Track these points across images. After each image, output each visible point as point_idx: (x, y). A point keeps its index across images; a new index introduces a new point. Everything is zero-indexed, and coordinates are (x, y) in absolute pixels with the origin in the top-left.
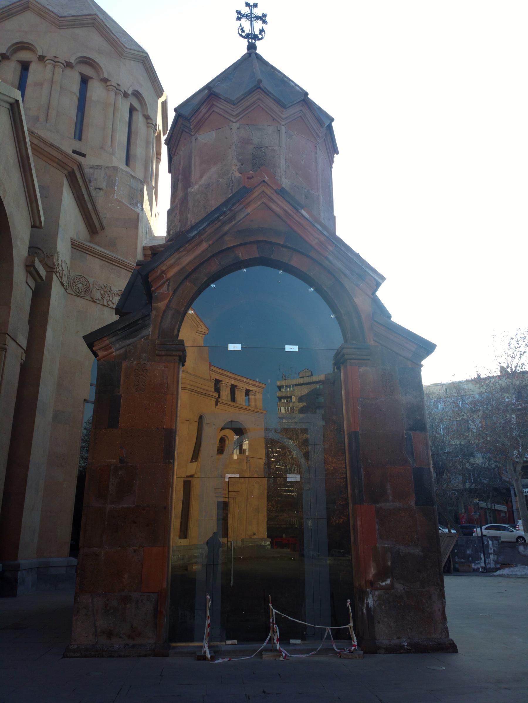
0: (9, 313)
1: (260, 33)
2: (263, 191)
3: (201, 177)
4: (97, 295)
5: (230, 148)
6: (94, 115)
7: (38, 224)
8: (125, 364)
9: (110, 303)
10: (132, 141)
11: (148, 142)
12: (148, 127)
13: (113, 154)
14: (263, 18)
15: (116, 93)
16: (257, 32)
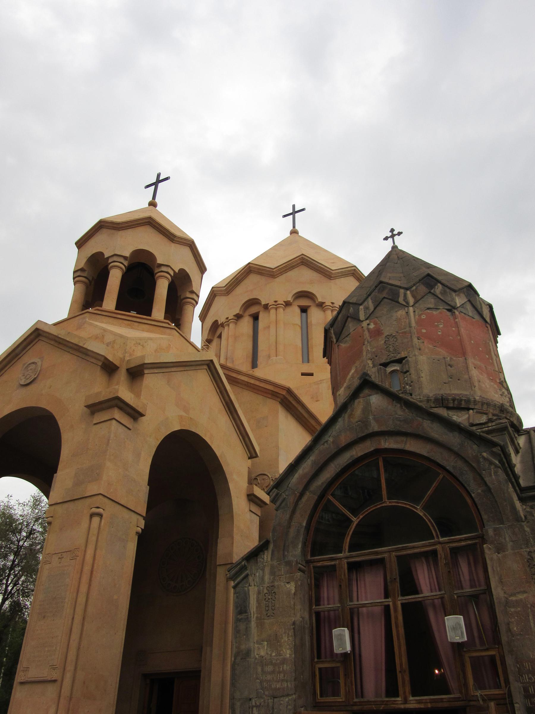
5: (364, 344)
7: (254, 455)
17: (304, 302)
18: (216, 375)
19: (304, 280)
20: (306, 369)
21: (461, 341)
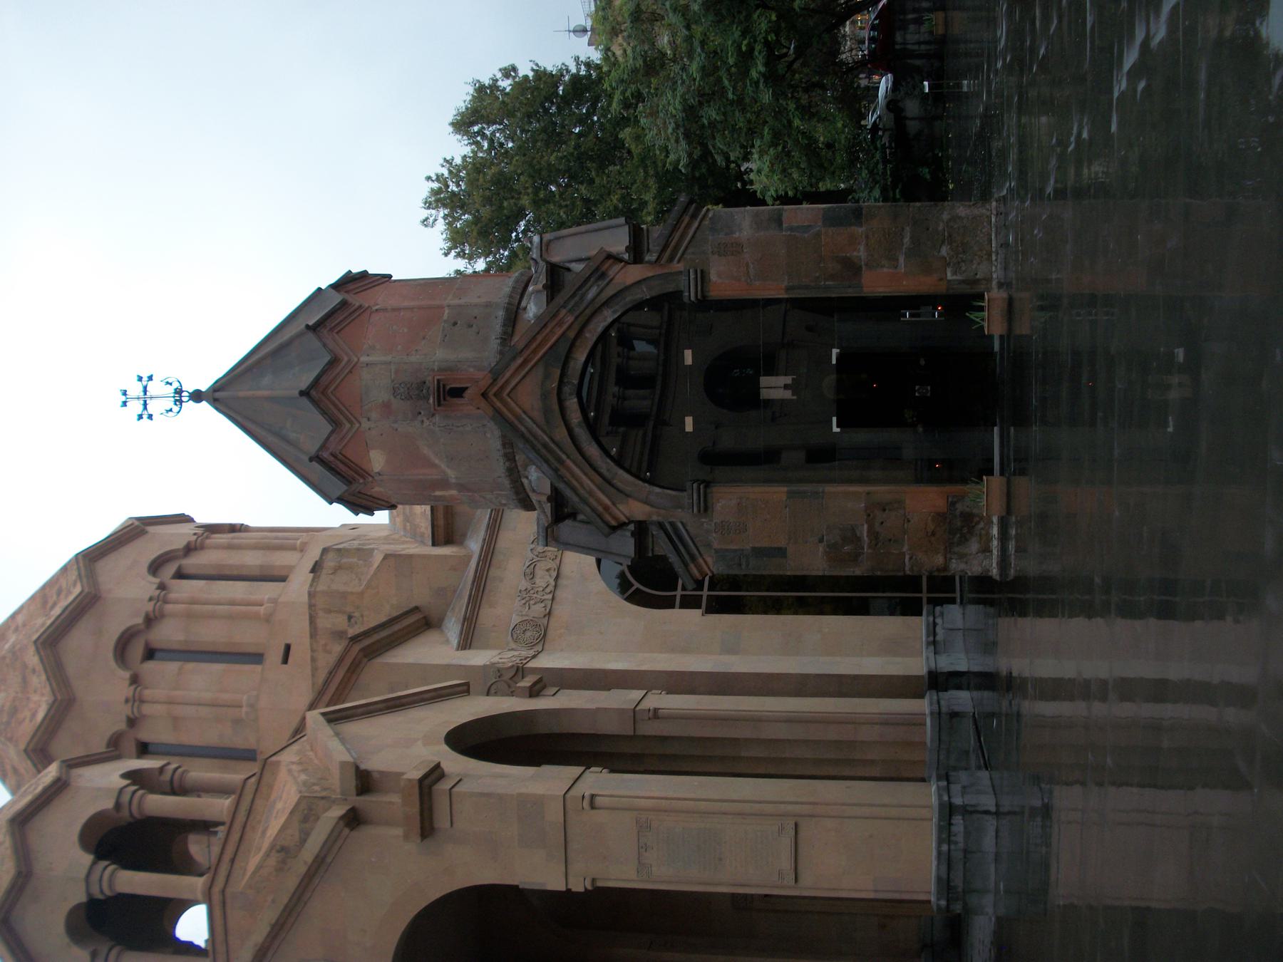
2: (495, 395)
3: (434, 466)
4: (538, 609)
6: (211, 634)
8: (716, 545)
9: (548, 590)
10: (235, 573)
11: (230, 547)
12: (202, 547)
13: (274, 601)
15: (166, 602)
17: (137, 650)
18: (344, 714)
19: (90, 645)
20: (275, 656)
21: (420, 308)
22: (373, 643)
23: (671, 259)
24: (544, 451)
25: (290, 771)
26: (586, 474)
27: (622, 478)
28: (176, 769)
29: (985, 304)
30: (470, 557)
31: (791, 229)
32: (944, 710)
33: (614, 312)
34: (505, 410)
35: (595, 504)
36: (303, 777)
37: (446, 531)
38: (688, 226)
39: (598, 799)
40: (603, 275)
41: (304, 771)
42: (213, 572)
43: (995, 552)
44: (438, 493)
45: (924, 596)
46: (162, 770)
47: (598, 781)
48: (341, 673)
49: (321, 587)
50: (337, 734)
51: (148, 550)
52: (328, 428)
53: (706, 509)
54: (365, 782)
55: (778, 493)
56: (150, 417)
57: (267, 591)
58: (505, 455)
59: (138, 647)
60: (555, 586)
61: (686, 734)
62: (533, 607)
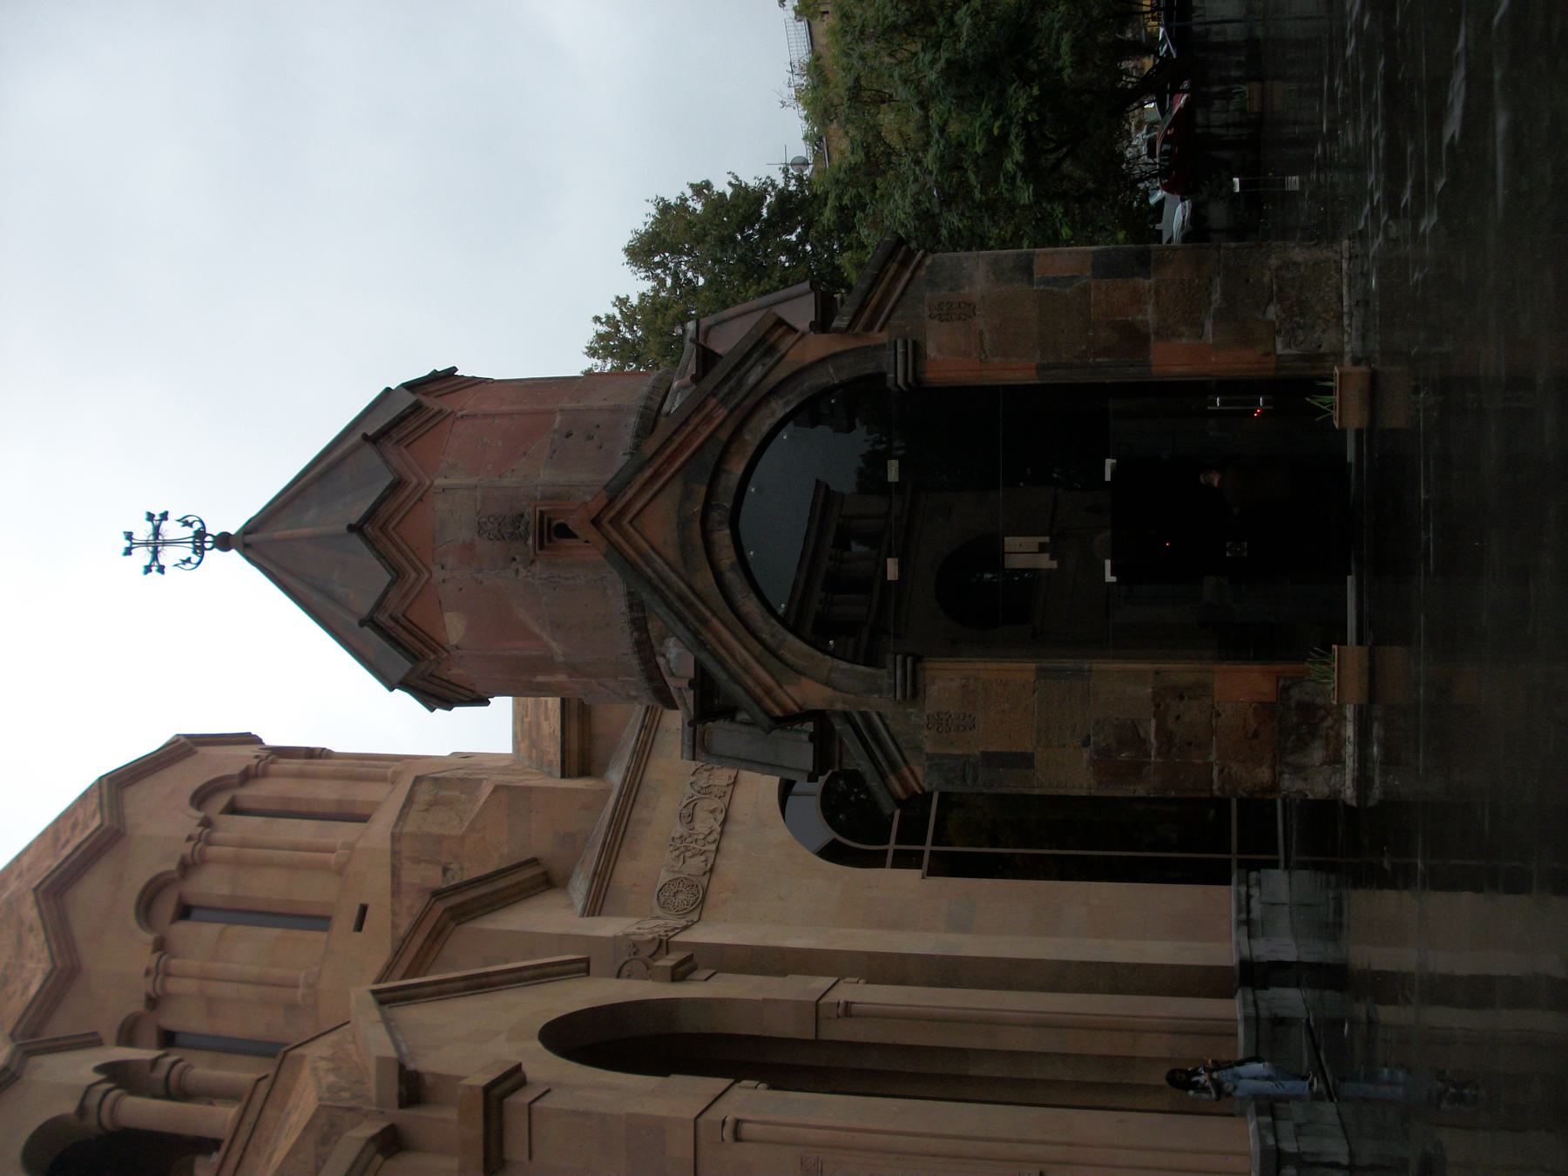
0: (776, 1001)
1: (191, 525)
2: (610, 522)
4: (696, 864)
6: (267, 887)
8: (928, 749)
9: (711, 838)
10: (305, 809)
13: (350, 847)
14: (157, 520)
15: (209, 843)
16: (189, 532)
17: (167, 905)
19: (106, 896)
20: (345, 919)
22: (464, 903)
23: (869, 327)
24: (678, 604)
25: (315, 1069)
26: (739, 640)
27: (794, 647)
28: (174, 1064)
29: (1335, 384)
30: (608, 792)
31: (1047, 282)
32: (1264, 1013)
33: (786, 404)
34: (626, 547)
35: (750, 683)
36: (331, 1078)
37: (580, 758)
38: (896, 278)
39: (746, 1126)
40: (772, 349)
41: (335, 1070)
42: (273, 807)
43: (1350, 763)
44: (541, 679)
45: (1234, 857)
46: (154, 1063)
47: (750, 1101)
48: (418, 940)
49: (409, 828)
50: (387, 1021)
51: (194, 774)
52: (385, 578)
53: (914, 692)
54: (413, 1088)
55: (1021, 670)
56: (161, 569)
57: (344, 833)
58: (633, 622)
59: (168, 902)
60: (722, 833)
61: (890, 1041)
62: (689, 861)
